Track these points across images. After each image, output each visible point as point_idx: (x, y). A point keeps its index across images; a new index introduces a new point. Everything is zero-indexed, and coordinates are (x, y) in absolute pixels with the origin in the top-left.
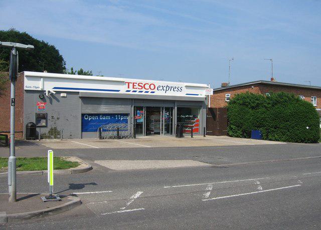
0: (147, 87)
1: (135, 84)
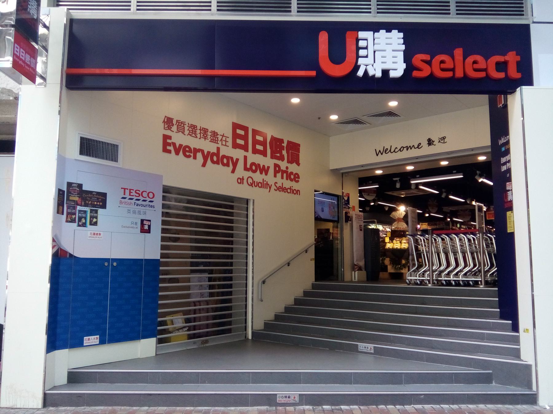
0: (145, 194)
1: (132, 191)
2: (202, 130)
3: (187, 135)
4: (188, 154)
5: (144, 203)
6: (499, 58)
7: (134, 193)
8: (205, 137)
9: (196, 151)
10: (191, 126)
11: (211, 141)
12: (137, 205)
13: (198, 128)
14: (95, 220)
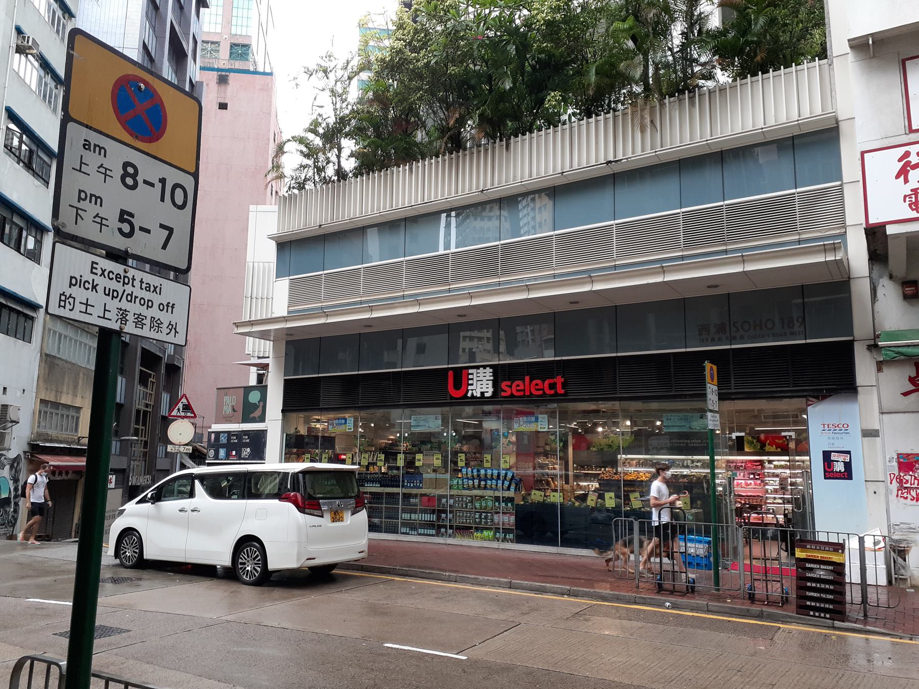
6: (552, 381)
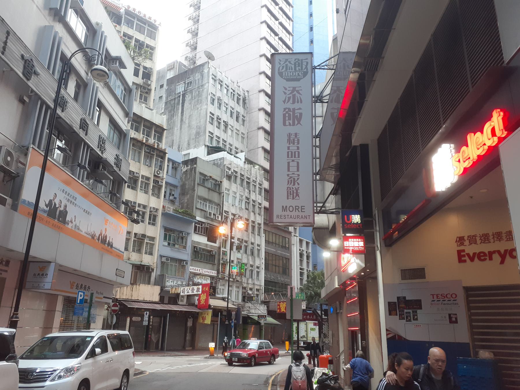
0: (449, 296)
1: (438, 295)
2: (496, 234)
3: (480, 243)
4: (482, 258)
5: (448, 302)
7: (440, 296)
8: (499, 239)
9: (491, 254)
10: (483, 236)
11: (507, 240)
12: (444, 304)
13: (491, 234)
14: (416, 317)
